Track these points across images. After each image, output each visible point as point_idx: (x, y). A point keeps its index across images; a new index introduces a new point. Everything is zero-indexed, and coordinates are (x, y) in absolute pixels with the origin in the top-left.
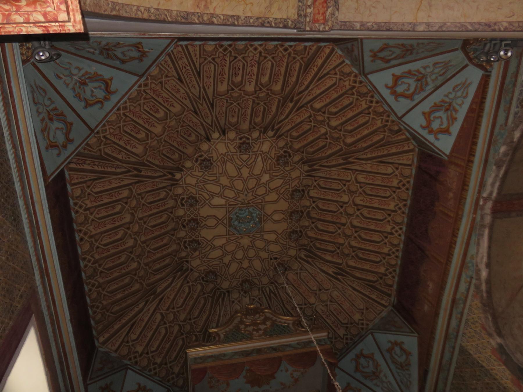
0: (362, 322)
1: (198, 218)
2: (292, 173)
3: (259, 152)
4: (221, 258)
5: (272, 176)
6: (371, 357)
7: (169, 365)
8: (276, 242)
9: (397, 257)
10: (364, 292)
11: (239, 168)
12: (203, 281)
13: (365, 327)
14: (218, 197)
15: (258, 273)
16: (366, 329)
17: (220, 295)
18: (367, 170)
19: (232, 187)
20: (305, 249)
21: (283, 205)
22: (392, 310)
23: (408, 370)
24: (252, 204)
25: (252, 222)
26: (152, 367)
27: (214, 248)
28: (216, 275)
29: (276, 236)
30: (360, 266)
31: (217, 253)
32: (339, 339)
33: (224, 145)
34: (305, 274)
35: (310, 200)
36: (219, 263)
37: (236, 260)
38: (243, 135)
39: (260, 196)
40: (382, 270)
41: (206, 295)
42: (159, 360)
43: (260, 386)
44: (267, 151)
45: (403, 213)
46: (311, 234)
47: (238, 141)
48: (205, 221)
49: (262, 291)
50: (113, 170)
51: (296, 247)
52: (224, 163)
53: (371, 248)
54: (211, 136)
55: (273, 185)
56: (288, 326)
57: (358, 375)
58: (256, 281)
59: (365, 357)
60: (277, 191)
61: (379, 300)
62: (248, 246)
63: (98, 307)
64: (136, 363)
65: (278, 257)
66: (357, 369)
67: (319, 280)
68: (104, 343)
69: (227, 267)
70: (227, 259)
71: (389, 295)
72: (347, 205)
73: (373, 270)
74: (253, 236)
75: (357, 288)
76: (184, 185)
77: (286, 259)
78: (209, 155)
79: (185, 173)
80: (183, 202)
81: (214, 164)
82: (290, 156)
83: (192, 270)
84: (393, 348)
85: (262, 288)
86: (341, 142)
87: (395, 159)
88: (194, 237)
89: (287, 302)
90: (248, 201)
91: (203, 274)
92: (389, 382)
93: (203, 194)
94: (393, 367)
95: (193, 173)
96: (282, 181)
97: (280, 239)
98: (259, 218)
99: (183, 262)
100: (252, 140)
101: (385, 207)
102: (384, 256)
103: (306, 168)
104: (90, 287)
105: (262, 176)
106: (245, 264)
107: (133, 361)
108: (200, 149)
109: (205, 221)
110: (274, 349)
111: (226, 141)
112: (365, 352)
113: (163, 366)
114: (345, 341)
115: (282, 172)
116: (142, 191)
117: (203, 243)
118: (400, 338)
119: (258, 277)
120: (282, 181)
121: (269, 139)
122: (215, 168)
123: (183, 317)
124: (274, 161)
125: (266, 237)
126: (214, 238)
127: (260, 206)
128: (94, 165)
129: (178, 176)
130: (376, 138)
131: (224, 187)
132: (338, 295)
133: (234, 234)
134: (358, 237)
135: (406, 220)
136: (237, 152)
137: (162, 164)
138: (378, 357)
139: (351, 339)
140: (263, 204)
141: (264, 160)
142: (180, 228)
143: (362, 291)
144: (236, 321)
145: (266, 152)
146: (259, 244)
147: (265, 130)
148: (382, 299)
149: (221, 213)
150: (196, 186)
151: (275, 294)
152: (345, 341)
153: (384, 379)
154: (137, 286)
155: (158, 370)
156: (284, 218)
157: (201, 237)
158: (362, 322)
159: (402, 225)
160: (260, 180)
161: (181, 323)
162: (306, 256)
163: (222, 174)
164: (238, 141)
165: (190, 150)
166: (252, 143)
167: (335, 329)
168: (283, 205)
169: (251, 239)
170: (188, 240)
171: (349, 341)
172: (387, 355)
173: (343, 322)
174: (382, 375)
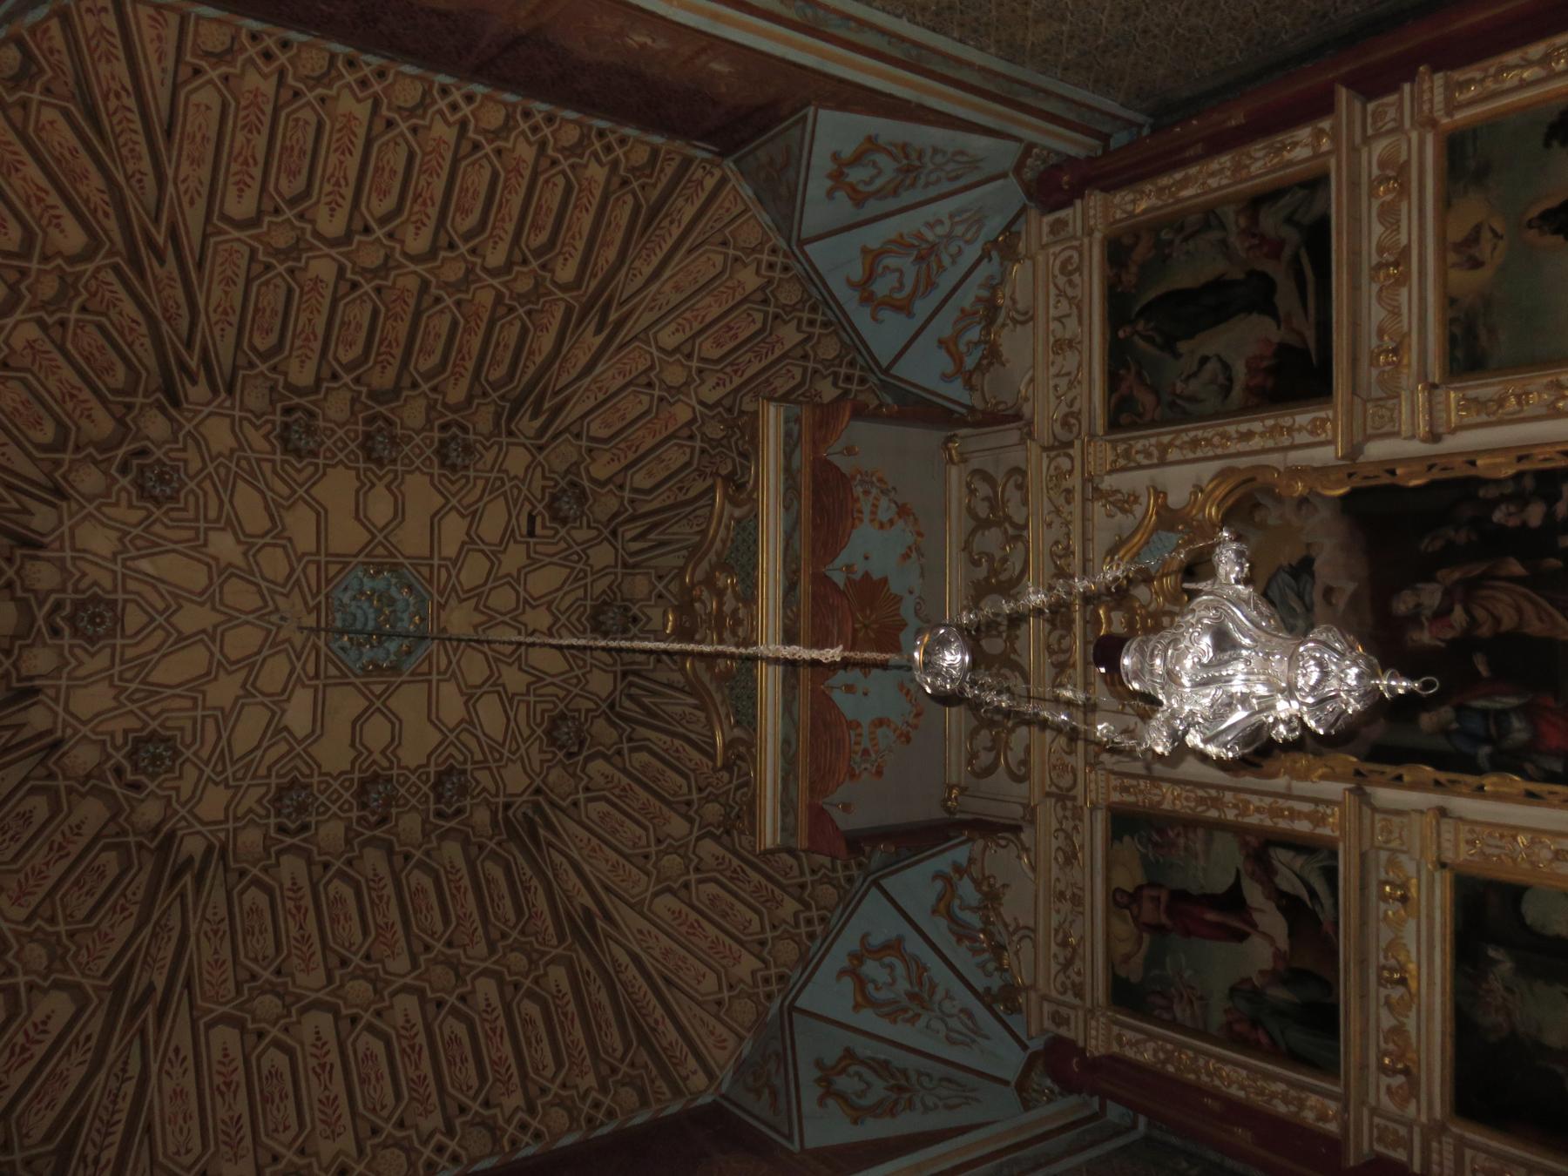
0: (764, 266)
1: (356, 775)
2: (215, 449)
3: (118, 568)
5: (218, 520)
6: (873, 258)
7: (808, 878)
8: (474, 516)
9: (550, 119)
10: (670, 242)
11: (176, 643)
12: (579, 753)
13: (779, 260)
14: (284, 711)
15: (576, 580)
16: (785, 255)
17: (630, 697)
18: (207, 182)
19: (251, 664)
20: (510, 419)
21: (337, 488)
22: (735, 162)
23: (920, 156)
24: (322, 598)
25: (394, 592)
26: (803, 929)
27: (470, 722)
28: (563, 716)
29: (454, 514)
30: (581, 245)
31: (491, 715)
32: (808, 348)
34: (594, 427)
35: (328, 389)
36: (523, 708)
38: (40, 622)
39: (293, 570)
40: (597, 173)
41: (625, 746)
42: (790, 906)
43: (903, 625)
44: (114, 535)
45: (381, 74)
46: (456, 394)
47: (67, 640)
48: (371, 753)
49: (635, 566)
50: (130, 1088)
53: (517, 201)
54: (40, 736)
56: (738, 521)
57: (923, 308)
58: (602, 585)
59: (870, 277)
60: (278, 505)
61: (703, 196)
62: (476, 609)
63: (597, 1105)
64: (782, 978)
65: (527, 507)
66: (904, 308)
67: (620, 381)
68: (711, 1076)
69: (540, 679)
71: (687, 162)
72: (349, 265)
73: (595, 202)
74: (441, 594)
75: (655, 261)
76: (230, 825)
77: (538, 483)
78: (119, 741)
79: (183, 823)
80: (292, 826)
81: (154, 725)
82: (143, 452)
83: (538, 791)
84: (853, 188)
85: (625, 565)
86: (79, 268)
87: (157, 72)
88: (425, 789)
89: (680, 489)
91: (555, 755)
92: (951, 216)
93: (267, 761)
94: (907, 198)
96: (240, 484)
97: (465, 502)
98: (378, 572)
99: (507, 820)
100: (63, 590)
101: (361, 132)
102: (545, 163)
103: (198, 392)
104: (526, 1139)
107: (774, 987)
108: (88, 776)
109: (371, 753)
110: (791, 587)
112: (857, 273)
113: (806, 896)
114: (817, 331)
115: (207, 485)
116: (230, 973)
117: (451, 756)
118: (821, 162)
119: (589, 580)
120: (240, 484)
121: (65, 528)
122: (169, 724)
123: (677, 826)
124: (157, 513)
125: (450, 550)
126: (434, 721)
127: (333, 569)
128: (96, 1161)
129: (193, 846)
130: (63, 136)
131: (248, 691)
132: (673, 326)
134: (471, 244)
135: (407, 69)
136: (114, 647)
137: (135, 909)
138: (874, 236)
139: (814, 309)
140: (323, 559)
142: (388, 831)
143: (666, 248)
144: (706, 678)
145: (120, 540)
147: (31, 543)
148: (701, 183)
149: (346, 703)
150: (239, 787)
151: (654, 526)
152: (817, 331)
153: (940, 230)
154: (558, 974)
155: (814, 914)
156: (388, 487)
157: (428, 765)
158: (764, 266)
159: (431, 84)
160: (230, 565)
161: (695, 834)
162: (535, 416)
163: (195, 699)
164: (67, 640)
165: (92, 812)
166: (76, 591)
167: (778, 353)
168: (337, 488)
169: (453, 602)
170: (432, 807)
171: (819, 318)
172: (873, 207)
173: (758, 325)
174: (930, 236)
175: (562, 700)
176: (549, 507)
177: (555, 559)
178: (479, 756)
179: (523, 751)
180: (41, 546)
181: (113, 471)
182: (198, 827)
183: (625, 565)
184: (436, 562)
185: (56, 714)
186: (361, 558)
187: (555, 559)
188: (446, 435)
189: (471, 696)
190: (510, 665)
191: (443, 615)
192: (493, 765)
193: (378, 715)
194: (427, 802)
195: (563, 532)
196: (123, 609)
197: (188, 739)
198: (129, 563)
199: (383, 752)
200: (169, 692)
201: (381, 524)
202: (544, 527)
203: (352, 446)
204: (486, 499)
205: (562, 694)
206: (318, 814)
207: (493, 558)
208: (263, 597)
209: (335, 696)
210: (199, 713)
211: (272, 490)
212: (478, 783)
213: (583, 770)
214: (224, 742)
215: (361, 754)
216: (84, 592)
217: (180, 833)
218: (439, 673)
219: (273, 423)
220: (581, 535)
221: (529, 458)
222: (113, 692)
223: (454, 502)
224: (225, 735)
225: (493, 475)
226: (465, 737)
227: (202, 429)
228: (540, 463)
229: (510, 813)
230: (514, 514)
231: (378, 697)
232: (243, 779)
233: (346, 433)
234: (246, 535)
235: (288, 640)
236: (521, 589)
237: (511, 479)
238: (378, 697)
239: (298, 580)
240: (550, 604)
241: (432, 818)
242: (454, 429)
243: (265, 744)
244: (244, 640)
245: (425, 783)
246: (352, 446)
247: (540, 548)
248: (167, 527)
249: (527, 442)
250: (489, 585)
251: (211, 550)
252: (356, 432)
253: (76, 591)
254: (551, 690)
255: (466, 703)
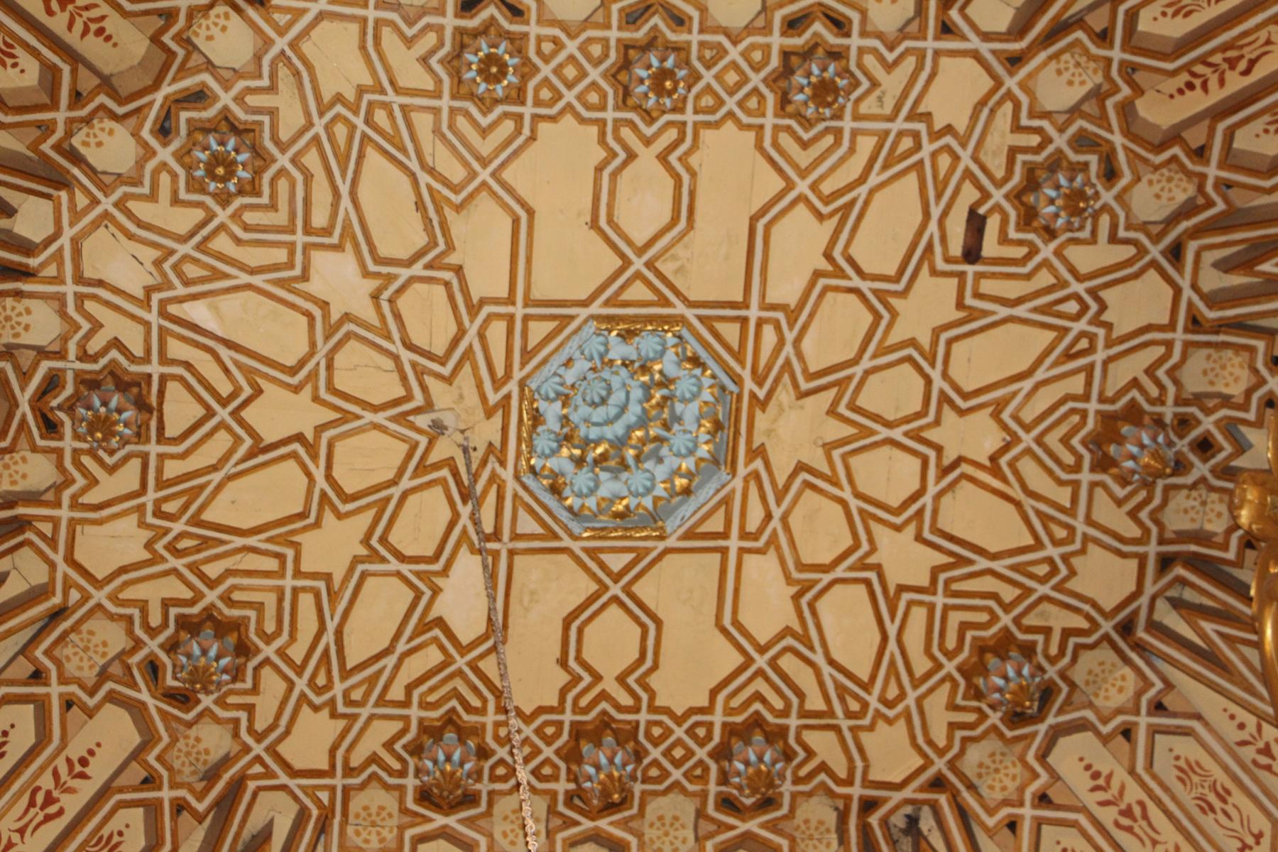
1: (568, 717)
3: (153, 317)
4: (887, 599)
8: (844, 213)
11: (250, 455)
14: (436, 591)
15: (1068, 356)
19: (382, 503)
21: (558, 164)
24: (512, 387)
27: (802, 637)
31: (848, 625)
33: (89, 529)
36: (919, 614)
37: (927, 499)
44: (150, 254)
51: (921, 55)
52: (211, 536)
55: (399, 231)
62: (832, 412)
65: (969, 195)
70: (905, 559)
76: (338, 781)
78: (155, 620)
79: (258, 769)
81: (211, 596)
85: (1195, 323)
88: (701, 753)
90: (489, 413)
93: (404, 678)
95: (260, 726)
97: (827, 188)
105: (324, 305)
106: (975, 437)
109: (597, 678)
111: (64, 513)
119: (1099, 356)
120: (372, 155)
121: (65, 241)
122: (236, 596)
124: (222, 215)
125: (785, 289)
126: (731, 629)
127: (538, 331)
131: (377, 547)
133: (727, 502)
140: (519, 311)
141: (214, 281)
146: (836, 330)
149: (551, 587)
150: (353, 718)
156: (663, 158)
165: (111, 735)
166: (84, 356)
169: (785, 395)
175: (1007, 608)
176: (1017, 196)
177: (1021, 311)
178: (815, 702)
179: (910, 700)
180: (26, 274)
181: (146, 133)
182: (283, 779)
183: (1195, 323)
184: (753, 313)
185: (52, 566)
186: (595, 308)
187: (1021, 311)
188: (797, 42)
189: (805, 587)
190: (898, 528)
191: (762, 420)
192: (845, 724)
193: (614, 610)
194: (703, 778)
195: (1047, 251)
196: (161, 393)
197: (270, 627)
198: (173, 309)
199: (621, 679)
200: (239, 542)
201: (640, 238)
202: (1004, 240)
203: (594, 74)
204: (874, 180)
205: (1009, 593)
206: (493, 778)
207: (882, 300)
208: (404, 378)
209: (530, 570)
210: (288, 583)
211: (431, 171)
212: (810, 754)
213: (1043, 757)
214: (329, 638)
215: (577, 679)
216: (94, 358)
217: (252, 785)
218: (744, 535)
219: (440, 29)
220: (1086, 258)
221: (987, 83)
222: (146, 535)
223: (802, 187)
224: (331, 626)
225: (899, 124)
226: (787, 663)
227: (306, 47)
228: (1009, 95)
229: (874, 820)
230: (936, 212)
231: (616, 578)
232: (360, 704)
233: (583, 49)
234: (379, 261)
235: (450, 463)
236: (936, 374)
237: (935, 135)
238: (616, 578)
239: (469, 351)
240: (999, 406)
241: (711, 810)
242: (817, 26)
243: (401, 647)
244: (367, 458)
245: (702, 744)
246: (594, 74)
247: (987, 286)
248: (238, 241)
249: (985, 48)
250: (866, 363)
251: (313, 287)
252: (605, 42)
253: (84, 356)
254: (988, 584)
255: (796, 598)
